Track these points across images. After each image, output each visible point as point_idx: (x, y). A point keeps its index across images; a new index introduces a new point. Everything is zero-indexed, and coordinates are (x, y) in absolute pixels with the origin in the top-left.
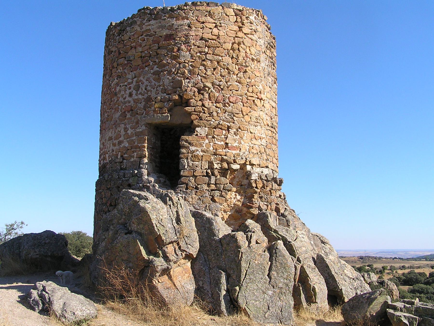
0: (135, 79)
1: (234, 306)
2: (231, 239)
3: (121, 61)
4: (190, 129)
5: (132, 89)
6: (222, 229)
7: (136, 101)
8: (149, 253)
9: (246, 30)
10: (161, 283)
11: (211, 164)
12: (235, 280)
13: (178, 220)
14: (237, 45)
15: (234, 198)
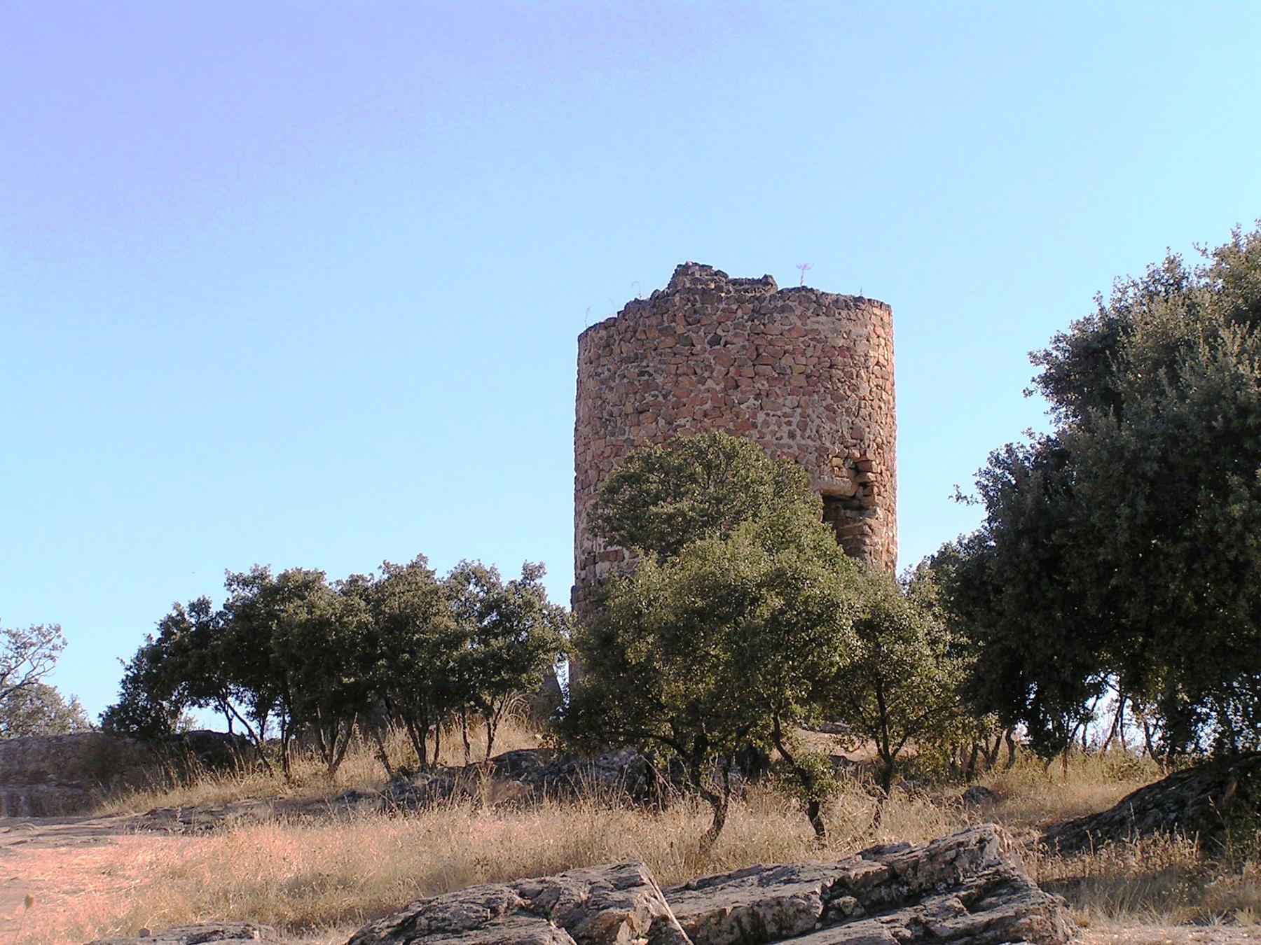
0: (799, 410)
5: (794, 427)
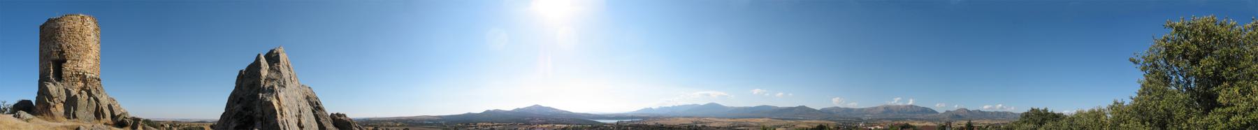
1: (75, 116)
4: (65, 61)
10: (52, 110)
12: (75, 109)
15: (81, 84)
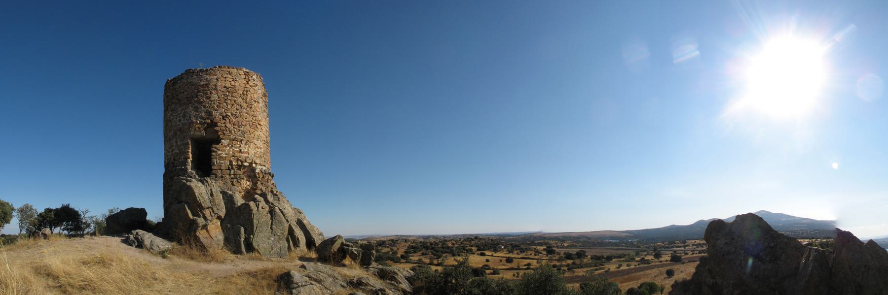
2: (246, 206)
3: (174, 101)
4: (218, 141)
6: (239, 201)
7: (184, 124)
8: (193, 215)
9: (251, 84)
10: (201, 234)
11: (231, 162)
12: (250, 231)
13: (212, 195)
14: (246, 92)
15: (246, 184)
